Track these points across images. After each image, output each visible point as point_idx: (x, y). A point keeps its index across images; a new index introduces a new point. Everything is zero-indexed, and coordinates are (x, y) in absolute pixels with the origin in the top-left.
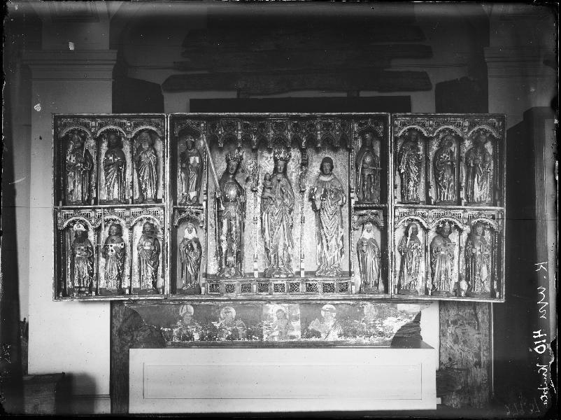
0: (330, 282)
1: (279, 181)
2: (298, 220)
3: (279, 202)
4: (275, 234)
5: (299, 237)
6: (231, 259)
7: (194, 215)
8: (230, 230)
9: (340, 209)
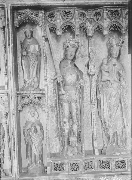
6: (73, 139)
8: (71, 113)
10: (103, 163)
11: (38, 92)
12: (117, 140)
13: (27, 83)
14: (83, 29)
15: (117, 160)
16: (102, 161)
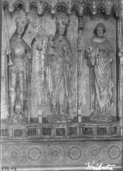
0: (104, 127)
2: (76, 75)
3: (60, 59)
4: (57, 86)
5: (76, 88)
9: (111, 66)
10: (45, 130)
12: (59, 110)
16: (45, 128)
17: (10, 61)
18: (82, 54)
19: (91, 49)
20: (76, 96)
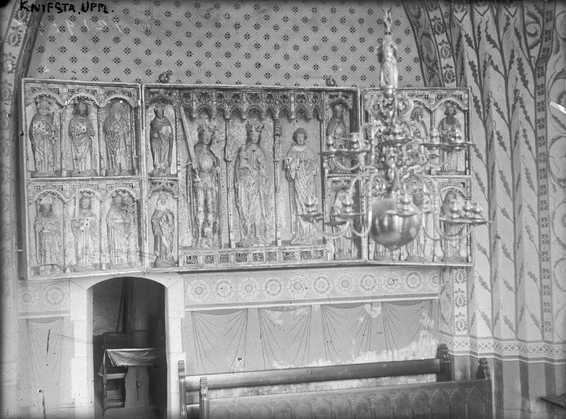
0: (307, 250)
1: (254, 151)
2: (272, 190)
3: (255, 173)
4: (252, 204)
5: (274, 206)
6: (208, 230)
7: (169, 186)
8: (206, 201)
11: (171, 178)
12: (255, 233)
13: (158, 167)
14: (221, 111)
15: (254, 252)
17: (198, 176)
18: (279, 166)
19: (291, 159)
20: (274, 215)
